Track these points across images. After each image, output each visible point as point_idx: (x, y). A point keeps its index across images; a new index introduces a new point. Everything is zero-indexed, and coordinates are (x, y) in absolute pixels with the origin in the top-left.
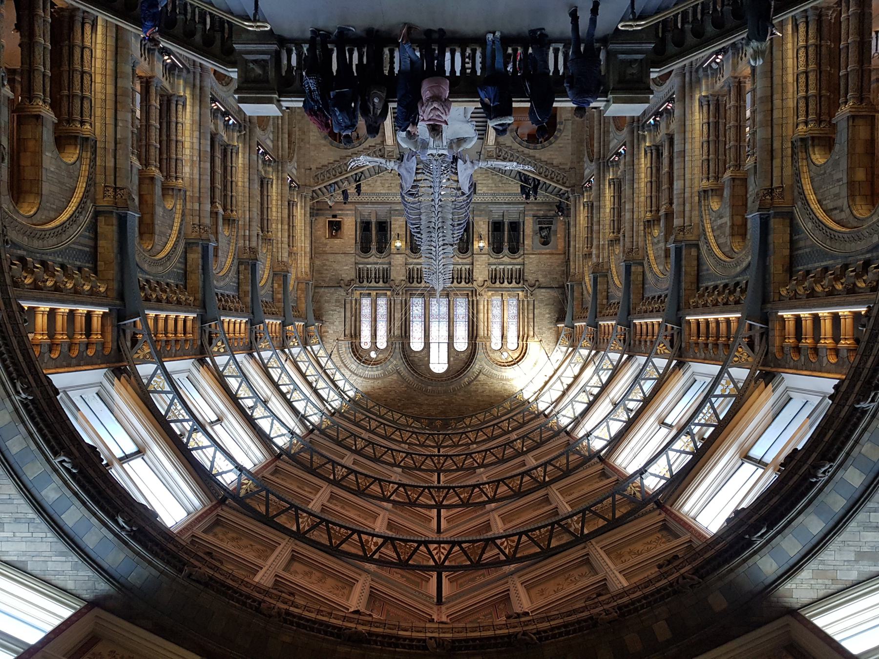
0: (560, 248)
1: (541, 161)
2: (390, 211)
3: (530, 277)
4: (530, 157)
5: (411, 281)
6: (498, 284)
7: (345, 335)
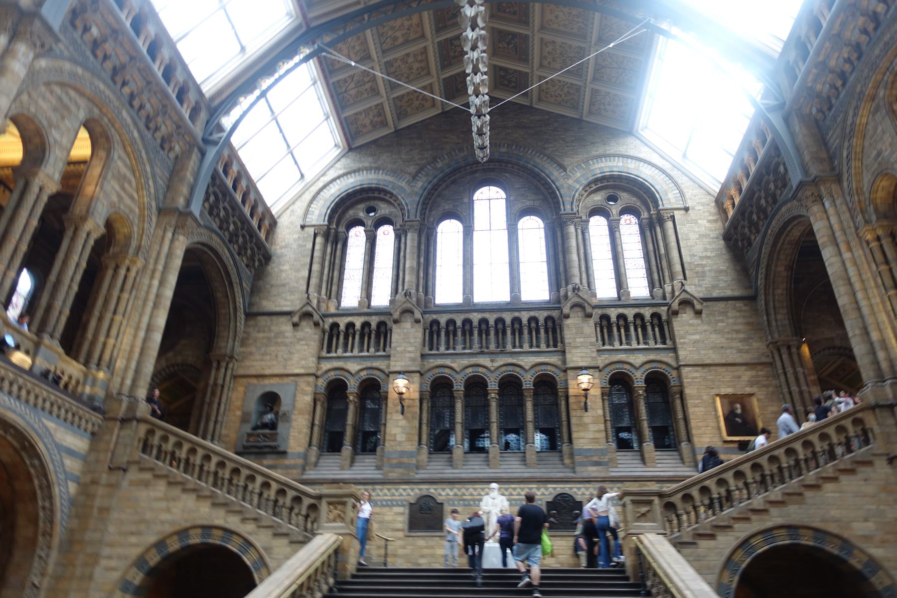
0: (241, 389)
2: (612, 463)
3: (308, 330)
6: (374, 321)
7: (673, 218)
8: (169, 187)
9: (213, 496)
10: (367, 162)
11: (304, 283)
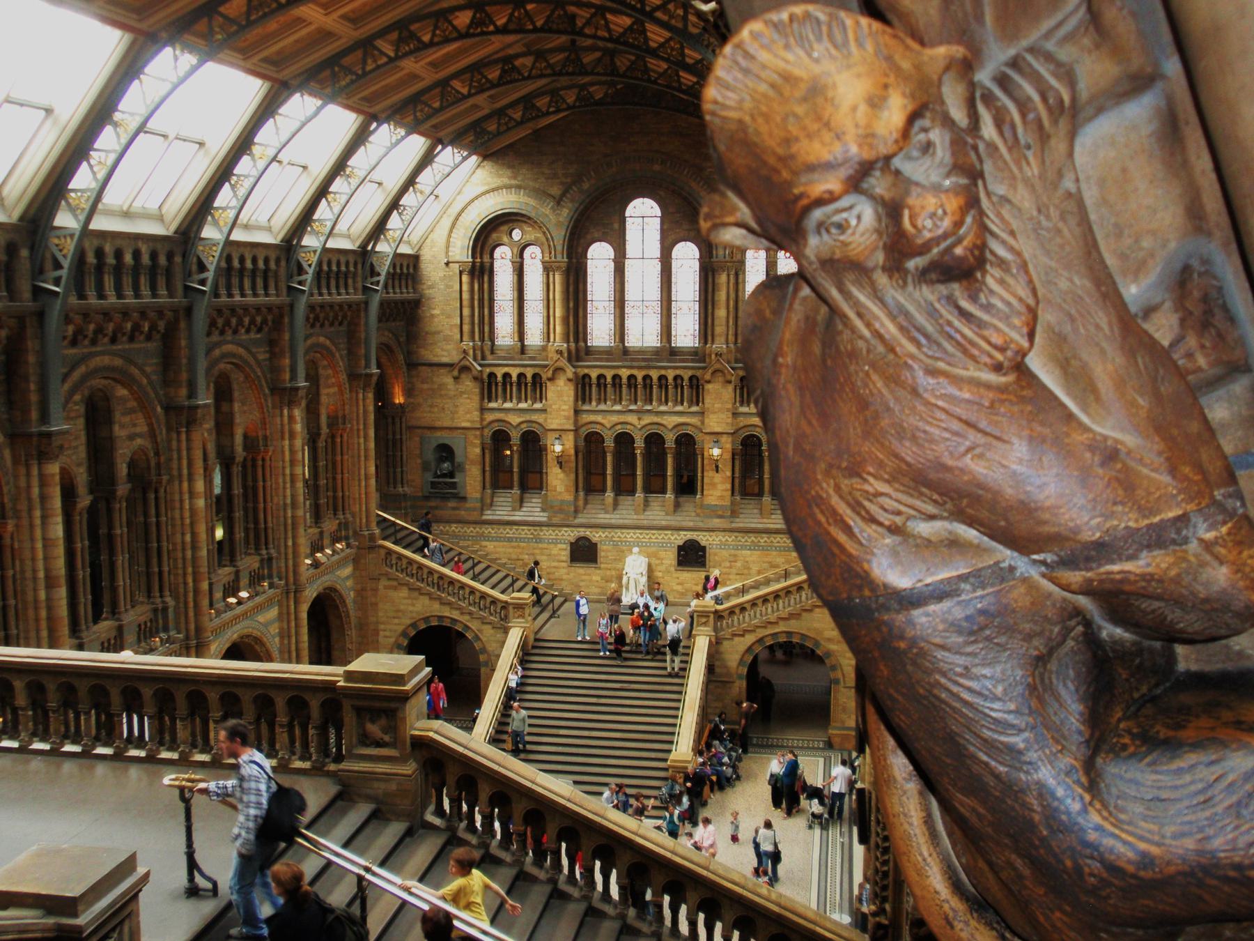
0: (417, 439)
1: (429, 595)
3: (468, 384)
4: (449, 604)
5: (695, 381)
6: (529, 373)
8: (351, 354)
9: (439, 599)
10: (504, 177)
11: (457, 331)
